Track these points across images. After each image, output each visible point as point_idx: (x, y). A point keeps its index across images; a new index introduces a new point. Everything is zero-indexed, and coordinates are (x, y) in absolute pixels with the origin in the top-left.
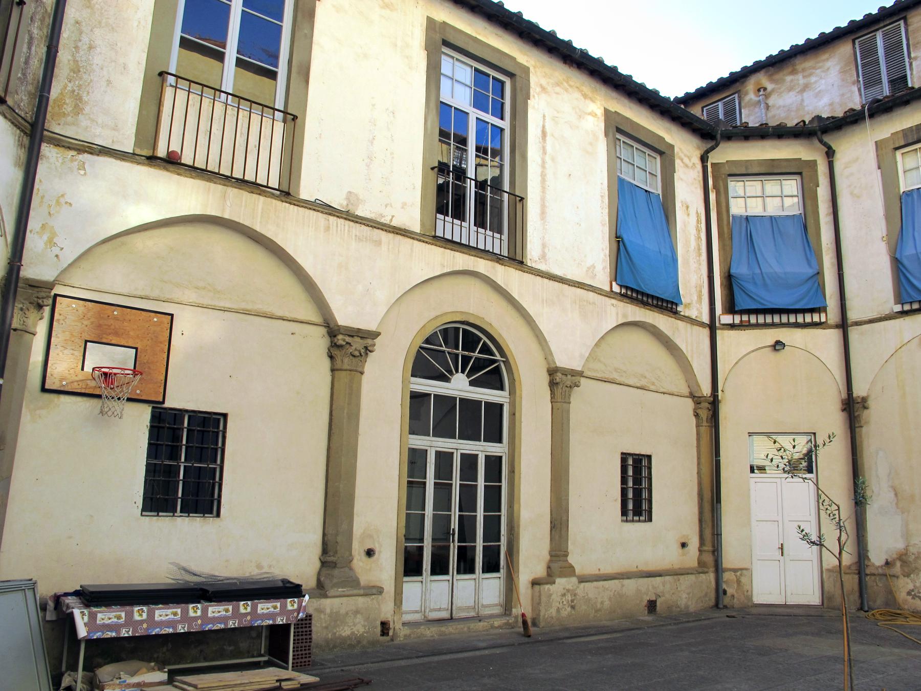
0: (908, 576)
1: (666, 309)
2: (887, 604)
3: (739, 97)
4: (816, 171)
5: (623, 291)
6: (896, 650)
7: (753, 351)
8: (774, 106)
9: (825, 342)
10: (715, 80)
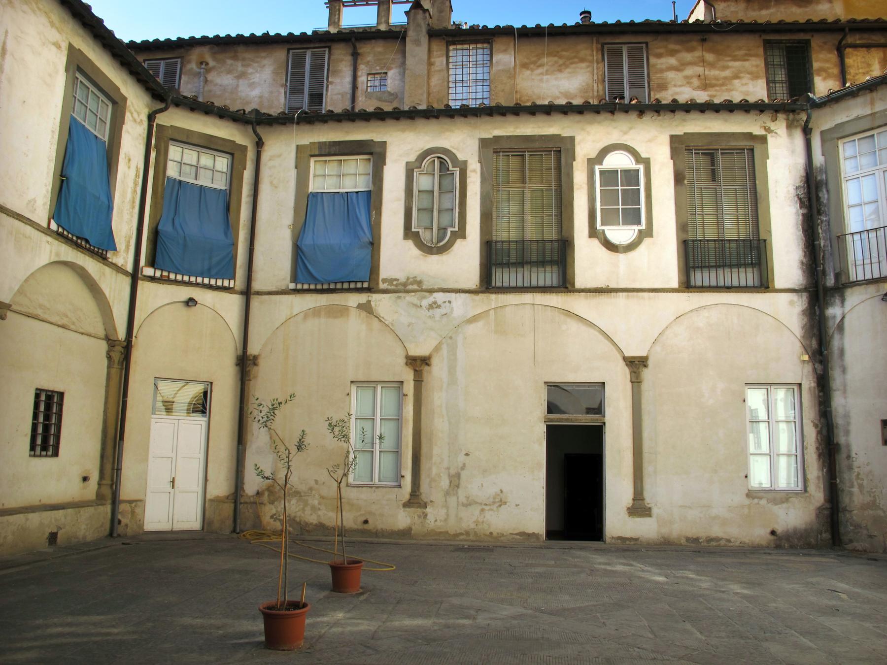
0: (272, 503)
1: (97, 254)
2: (254, 526)
3: (182, 63)
5: (60, 230)
6: (272, 560)
8: (211, 82)
9: (228, 305)
10: (162, 39)
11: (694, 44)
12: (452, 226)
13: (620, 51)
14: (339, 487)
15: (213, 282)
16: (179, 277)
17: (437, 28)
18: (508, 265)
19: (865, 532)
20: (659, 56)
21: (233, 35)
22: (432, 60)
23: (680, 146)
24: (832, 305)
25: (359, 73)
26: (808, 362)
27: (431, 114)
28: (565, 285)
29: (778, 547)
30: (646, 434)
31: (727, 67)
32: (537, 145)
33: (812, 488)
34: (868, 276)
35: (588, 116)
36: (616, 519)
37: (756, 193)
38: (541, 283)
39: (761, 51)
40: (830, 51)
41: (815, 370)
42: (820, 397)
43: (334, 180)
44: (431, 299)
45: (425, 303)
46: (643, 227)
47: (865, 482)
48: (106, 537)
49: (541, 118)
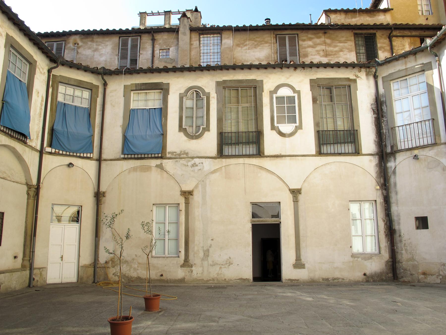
0: (114, 267)
3: (65, 43)
4: (98, 91)
6: (114, 296)
7: (59, 166)
9: (90, 167)
10: (55, 31)
11: (321, 35)
12: (203, 125)
13: (285, 38)
14: (148, 257)
15: (82, 155)
16: (64, 153)
17: (194, 27)
18: (231, 144)
19: (409, 272)
20: (304, 40)
21: (92, 30)
22: (192, 42)
23: (314, 84)
24: (390, 161)
25: (155, 49)
26: (379, 189)
27: (191, 69)
28: (260, 154)
29: (367, 281)
30: (301, 227)
31: (337, 46)
32: (244, 84)
33: (383, 252)
34: (407, 147)
35: (270, 70)
36: (288, 270)
37: (352, 107)
38: (248, 153)
39: (353, 38)
40: (385, 39)
41: (383, 193)
42: (385, 206)
43: (143, 102)
44: (193, 162)
45: (190, 164)
46: (298, 124)
47: (408, 248)
48: (27, 287)
49: (246, 71)
